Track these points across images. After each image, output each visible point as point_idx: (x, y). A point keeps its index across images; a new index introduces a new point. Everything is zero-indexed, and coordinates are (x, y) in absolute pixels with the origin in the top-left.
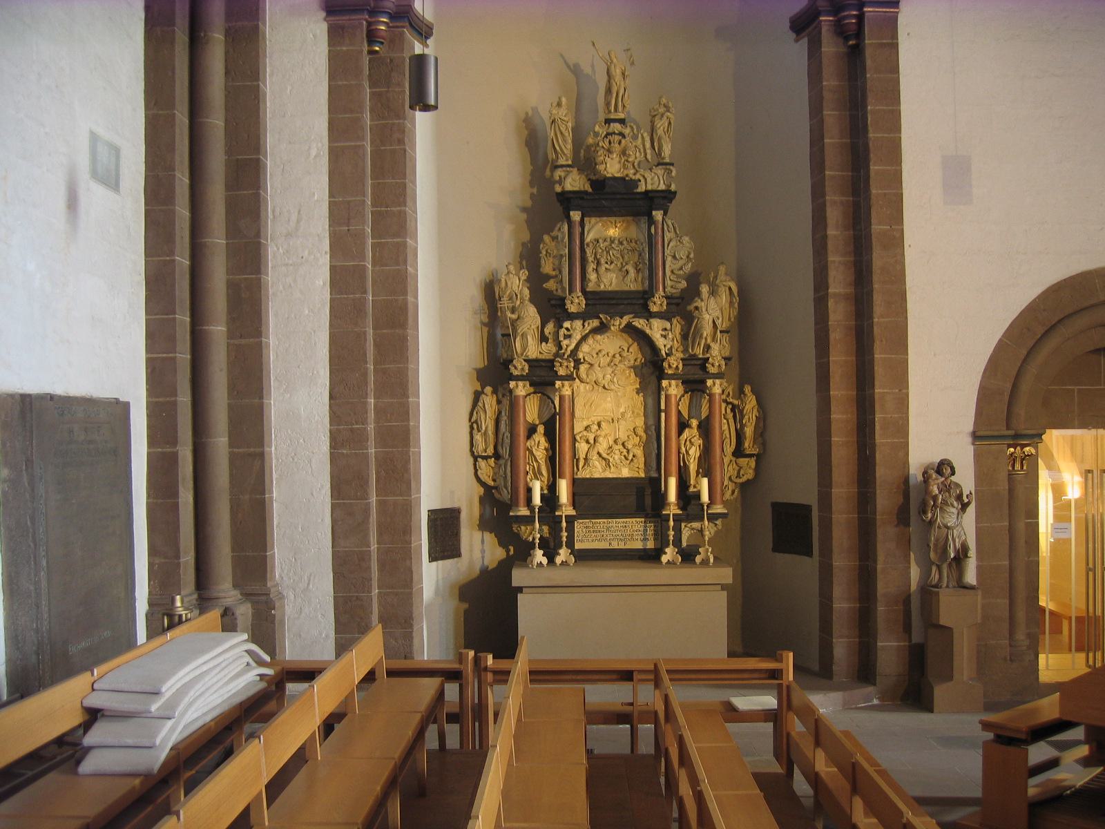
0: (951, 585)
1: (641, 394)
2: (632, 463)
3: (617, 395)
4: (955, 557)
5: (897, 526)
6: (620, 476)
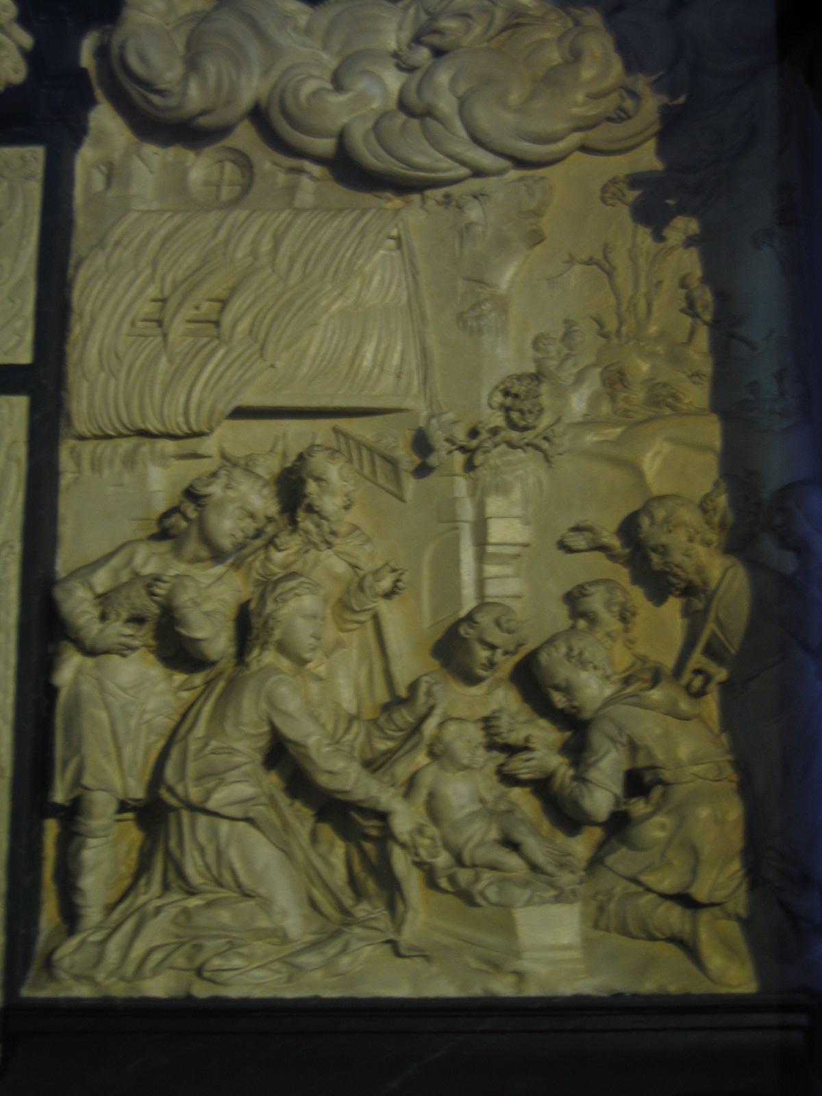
1: (684, 226)
2: (620, 859)
3: (464, 233)
6: (503, 987)
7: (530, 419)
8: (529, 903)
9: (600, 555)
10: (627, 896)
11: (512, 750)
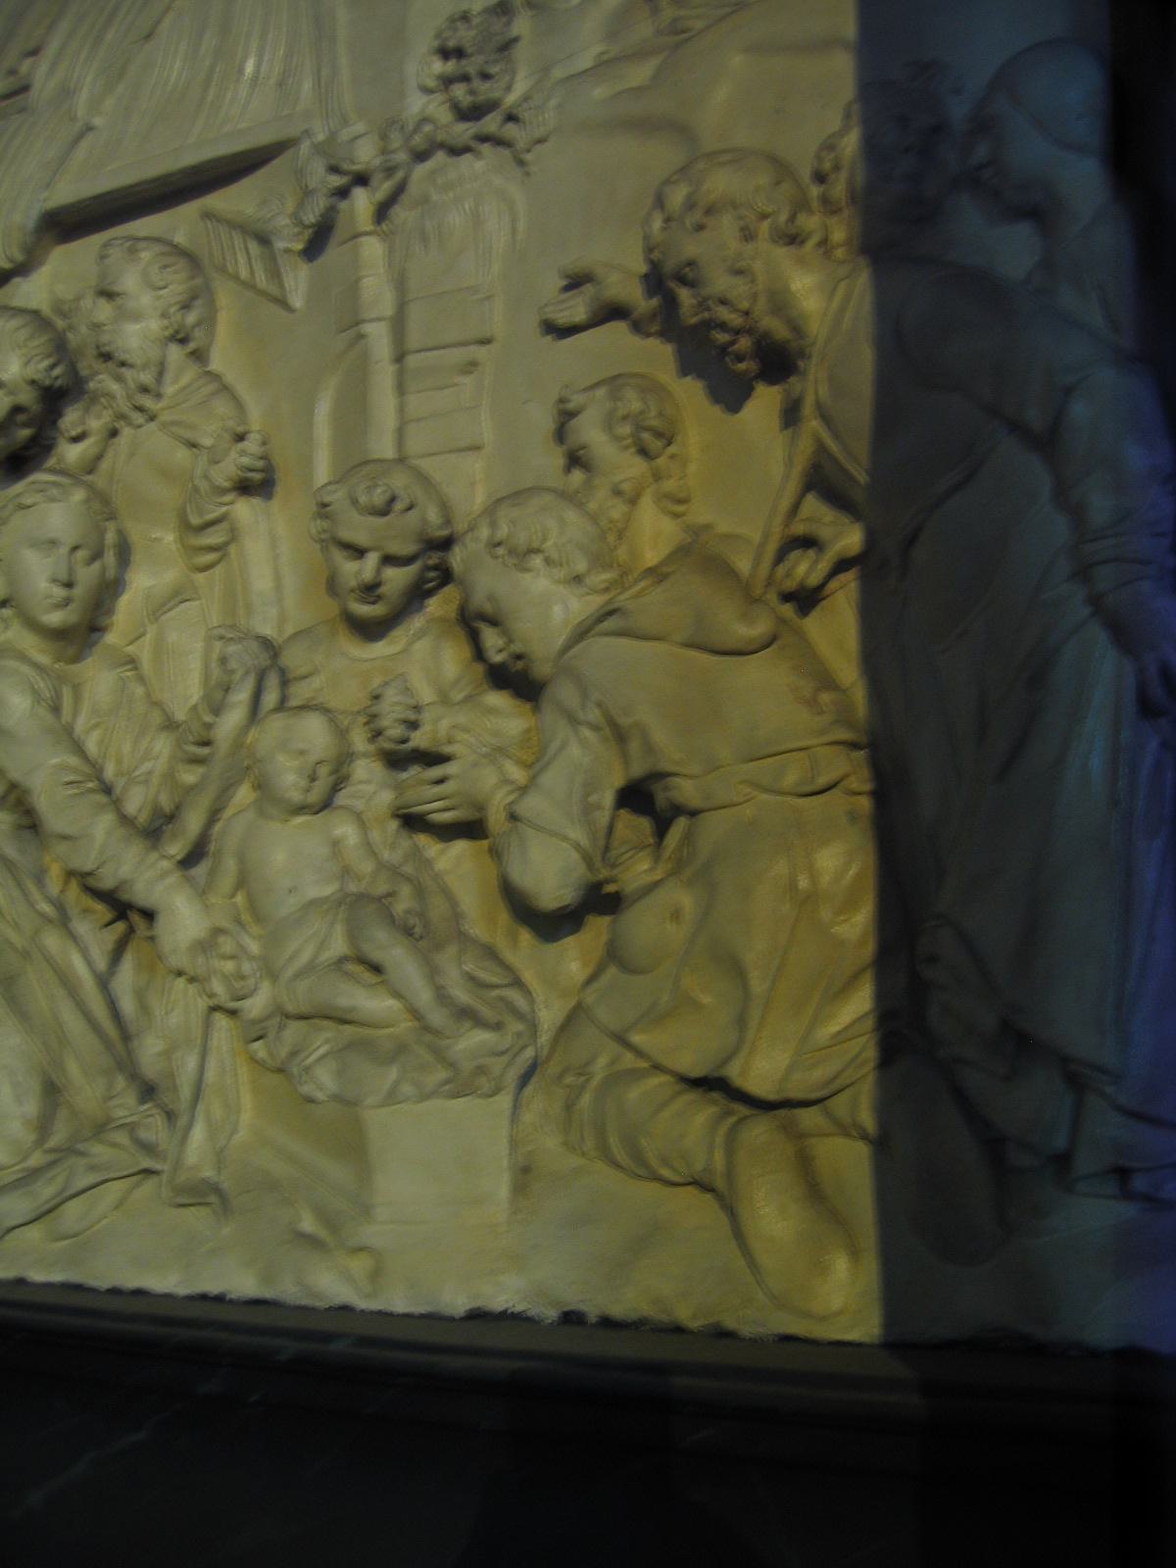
7: (485, 90)
8: (392, 1098)
9: (618, 329)
10: (618, 1078)
11: (431, 758)
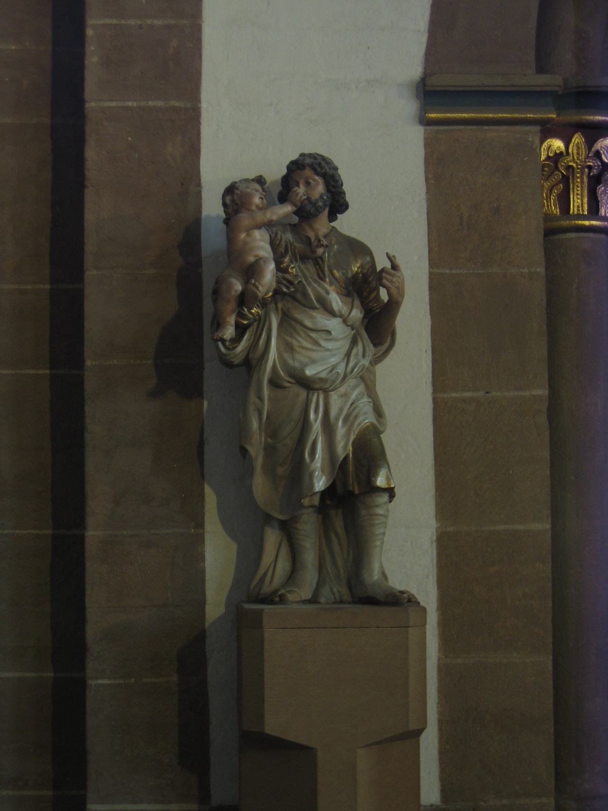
0: (326, 595)
4: (329, 492)
5: (154, 394)
